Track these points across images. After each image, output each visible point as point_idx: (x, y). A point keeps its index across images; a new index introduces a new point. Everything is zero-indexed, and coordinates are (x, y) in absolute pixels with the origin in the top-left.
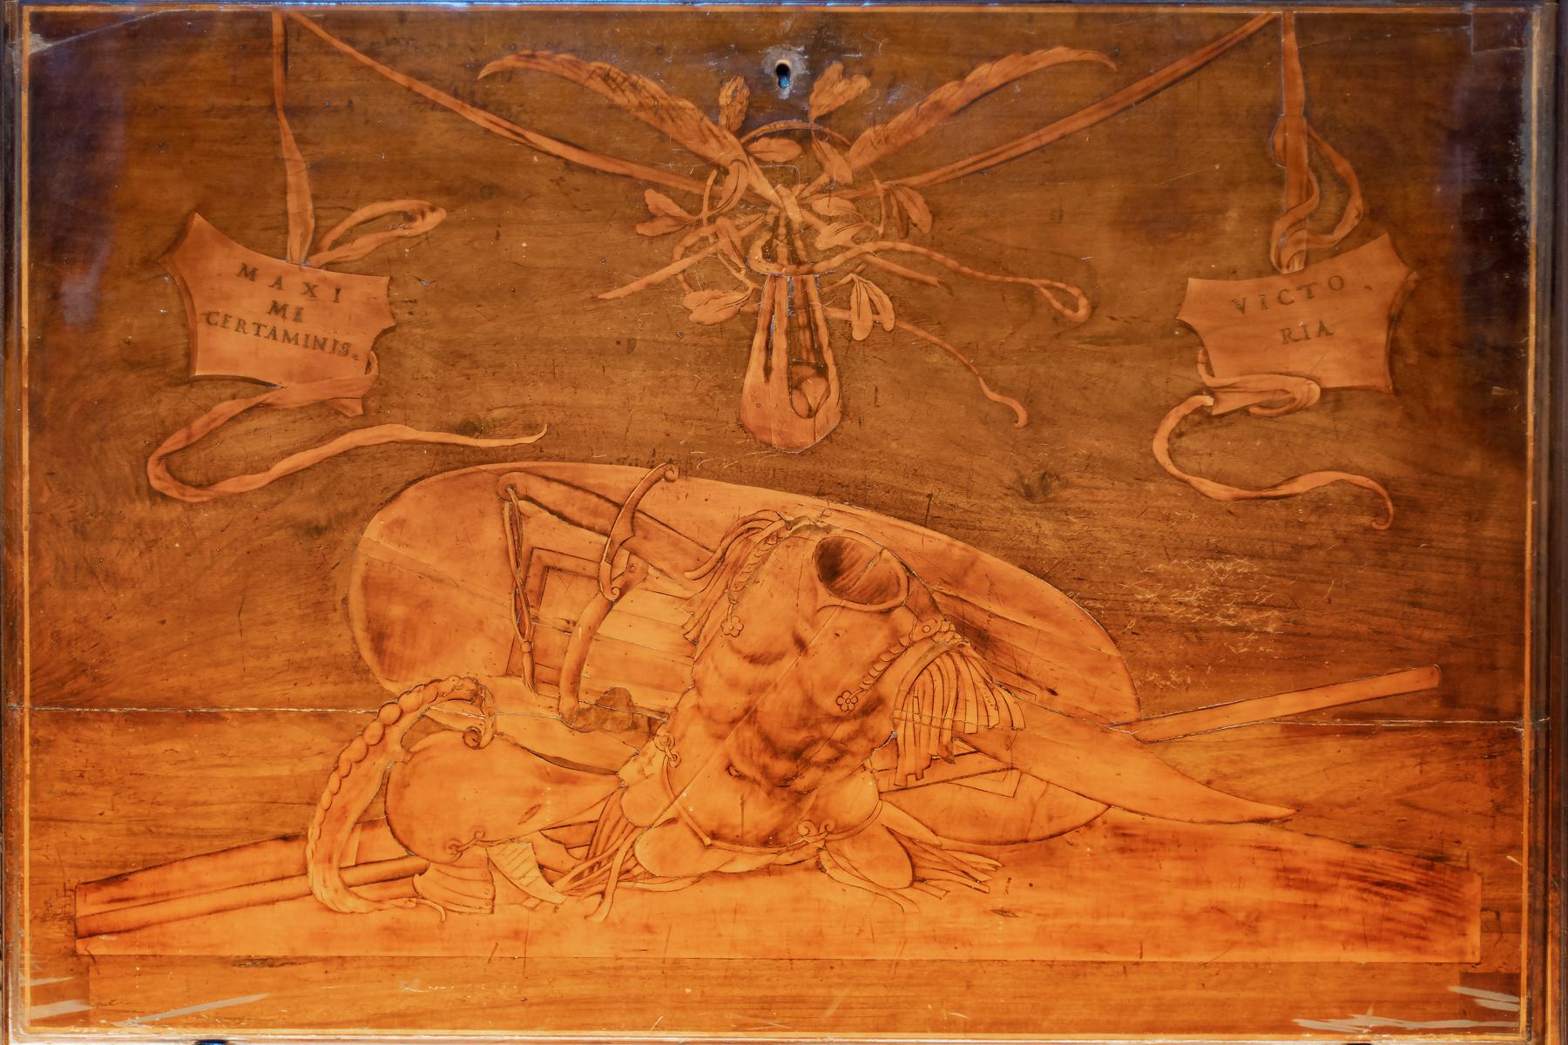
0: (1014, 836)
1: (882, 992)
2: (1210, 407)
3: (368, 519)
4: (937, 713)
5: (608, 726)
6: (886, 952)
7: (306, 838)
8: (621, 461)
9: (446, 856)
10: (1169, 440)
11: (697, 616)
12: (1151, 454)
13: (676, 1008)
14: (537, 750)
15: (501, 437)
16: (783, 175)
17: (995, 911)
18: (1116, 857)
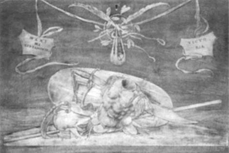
9: (63, 130)
16: (117, 22)
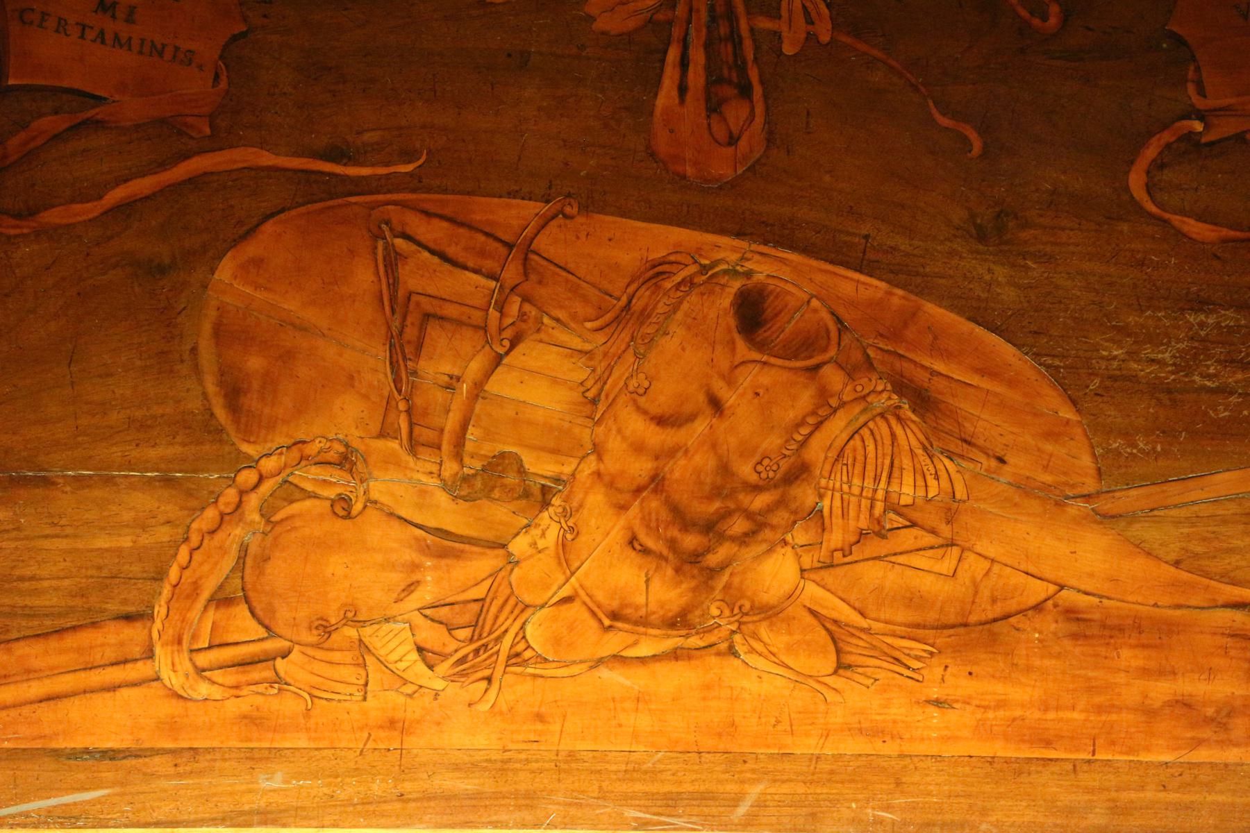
0: (952, 619)
1: (801, 789)
2: (1200, 133)
3: (220, 257)
4: (869, 483)
5: (496, 494)
6: (807, 745)
7: (151, 618)
8: (512, 194)
9: (312, 638)
10: (1148, 172)
11: (599, 371)
12: (1127, 189)
13: (570, 804)
14: (418, 521)
15: (373, 165)
17: (928, 702)
18: (1067, 643)
